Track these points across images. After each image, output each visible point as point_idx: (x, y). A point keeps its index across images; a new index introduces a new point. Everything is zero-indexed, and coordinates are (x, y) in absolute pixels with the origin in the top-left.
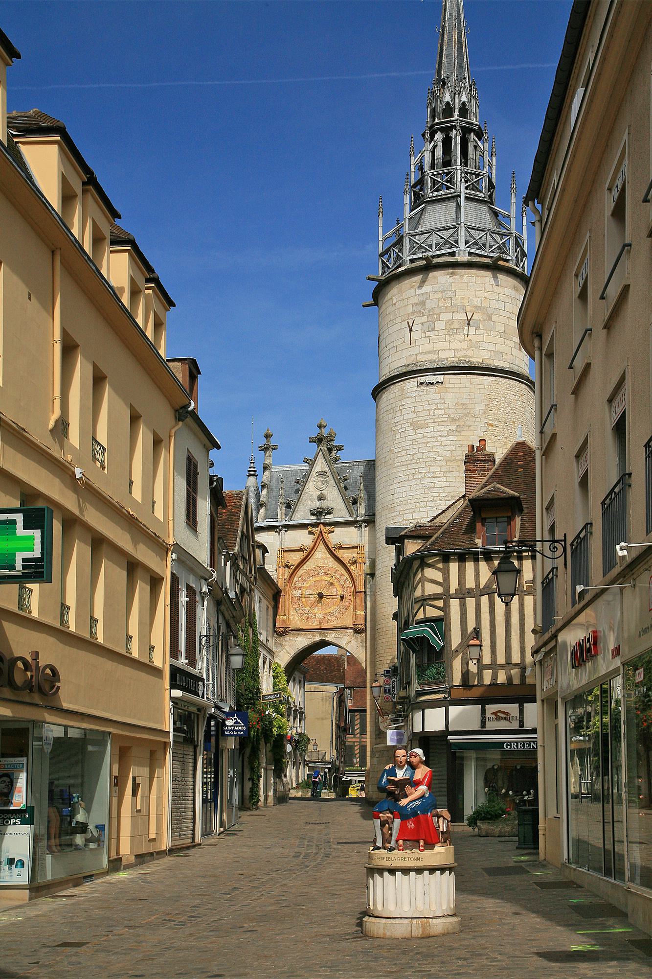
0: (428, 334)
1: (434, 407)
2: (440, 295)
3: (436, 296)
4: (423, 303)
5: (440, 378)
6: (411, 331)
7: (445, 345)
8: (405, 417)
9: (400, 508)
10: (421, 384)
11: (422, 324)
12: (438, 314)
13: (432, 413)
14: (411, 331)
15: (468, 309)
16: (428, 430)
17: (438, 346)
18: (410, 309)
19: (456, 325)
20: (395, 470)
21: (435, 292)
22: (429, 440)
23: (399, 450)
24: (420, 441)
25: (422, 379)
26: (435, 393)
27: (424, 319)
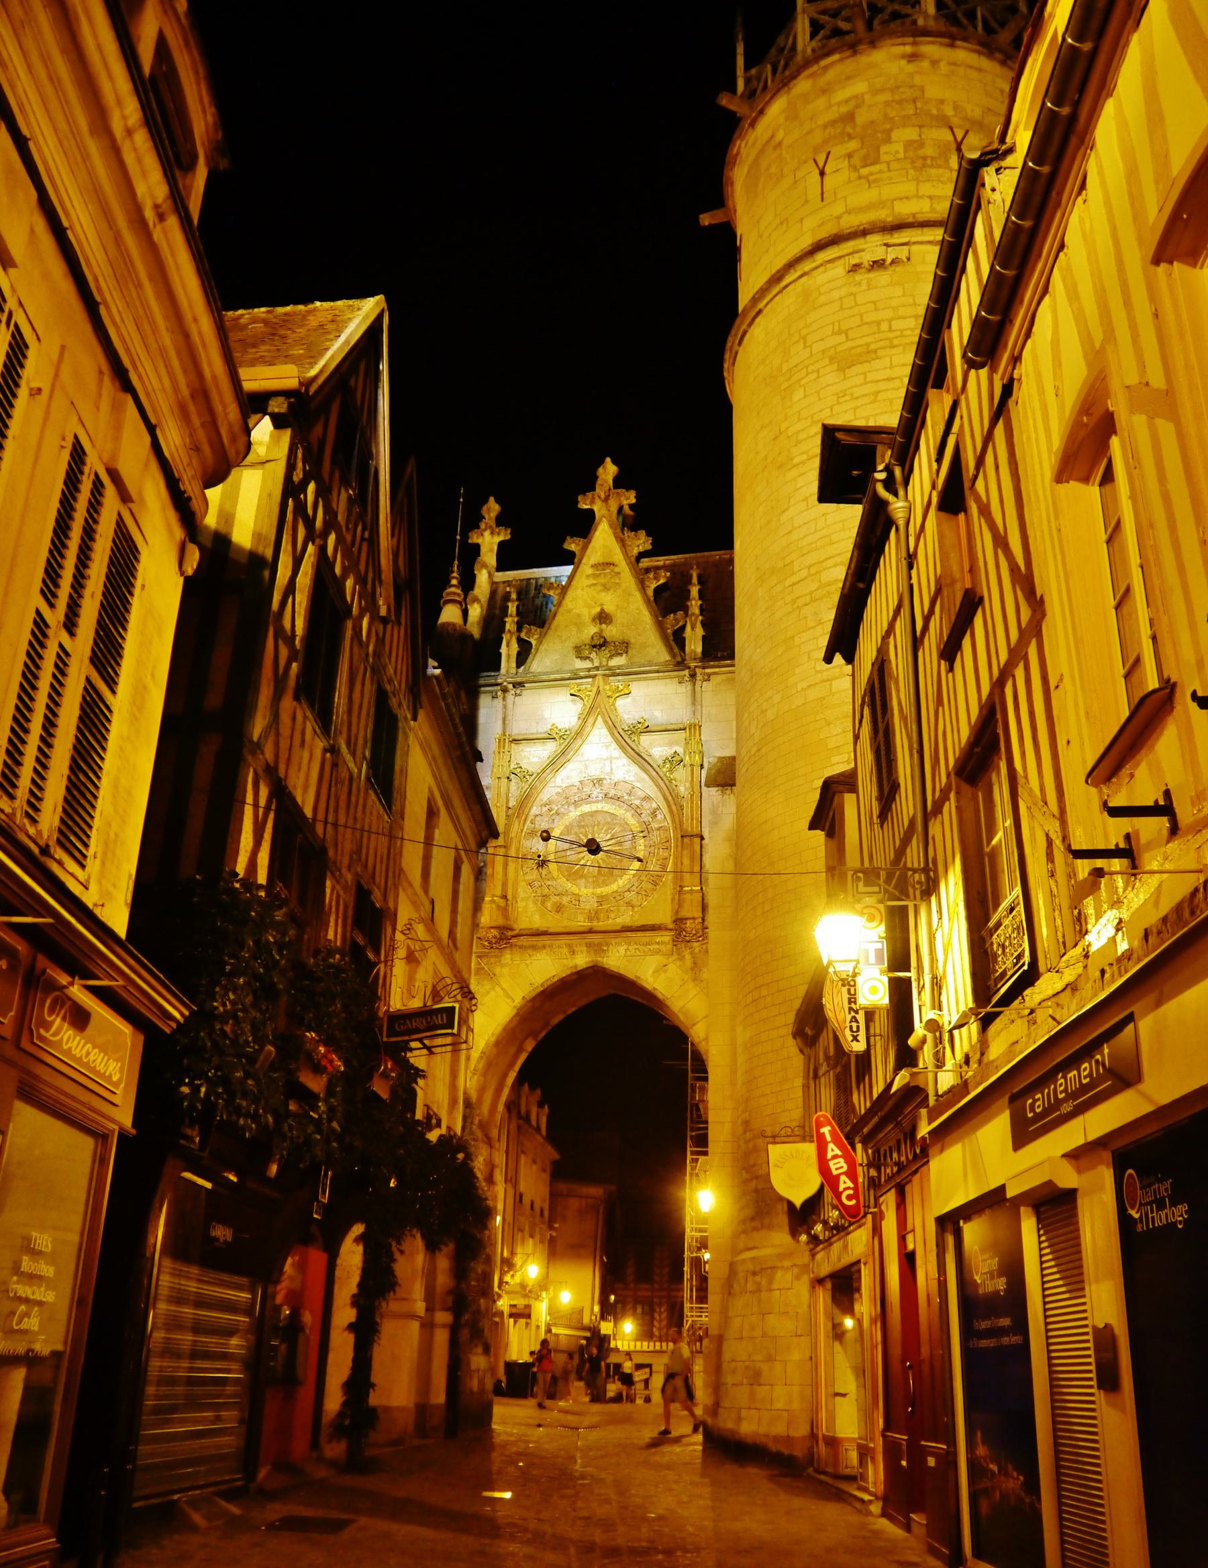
0: (865, 171)
1: (889, 314)
2: (887, 96)
3: (881, 98)
4: (850, 117)
5: (902, 253)
6: (822, 174)
7: (910, 188)
8: (817, 348)
9: (811, 559)
10: (855, 268)
11: (850, 156)
12: (888, 133)
13: (884, 326)
14: (822, 174)
15: (955, 121)
16: (876, 364)
17: (888, 192)
18: (817, 137)
19: (929, 151)
20: (793, 473)
21: (875, 92)
22: (882, 386)
23: (799, 426)
24: (858, 392)
25: (855, 260)
26: (891, 284)
27: (853, 145)
